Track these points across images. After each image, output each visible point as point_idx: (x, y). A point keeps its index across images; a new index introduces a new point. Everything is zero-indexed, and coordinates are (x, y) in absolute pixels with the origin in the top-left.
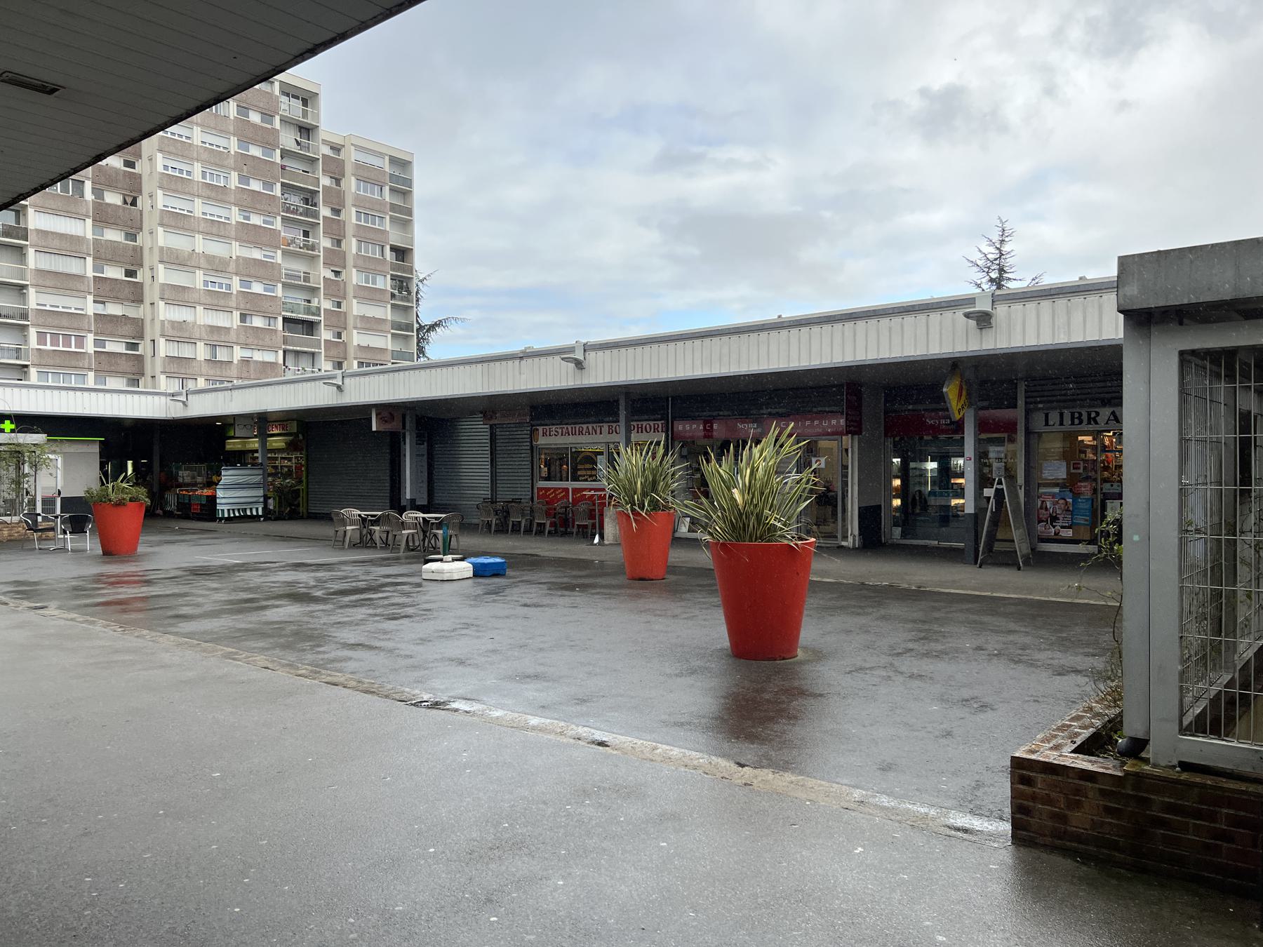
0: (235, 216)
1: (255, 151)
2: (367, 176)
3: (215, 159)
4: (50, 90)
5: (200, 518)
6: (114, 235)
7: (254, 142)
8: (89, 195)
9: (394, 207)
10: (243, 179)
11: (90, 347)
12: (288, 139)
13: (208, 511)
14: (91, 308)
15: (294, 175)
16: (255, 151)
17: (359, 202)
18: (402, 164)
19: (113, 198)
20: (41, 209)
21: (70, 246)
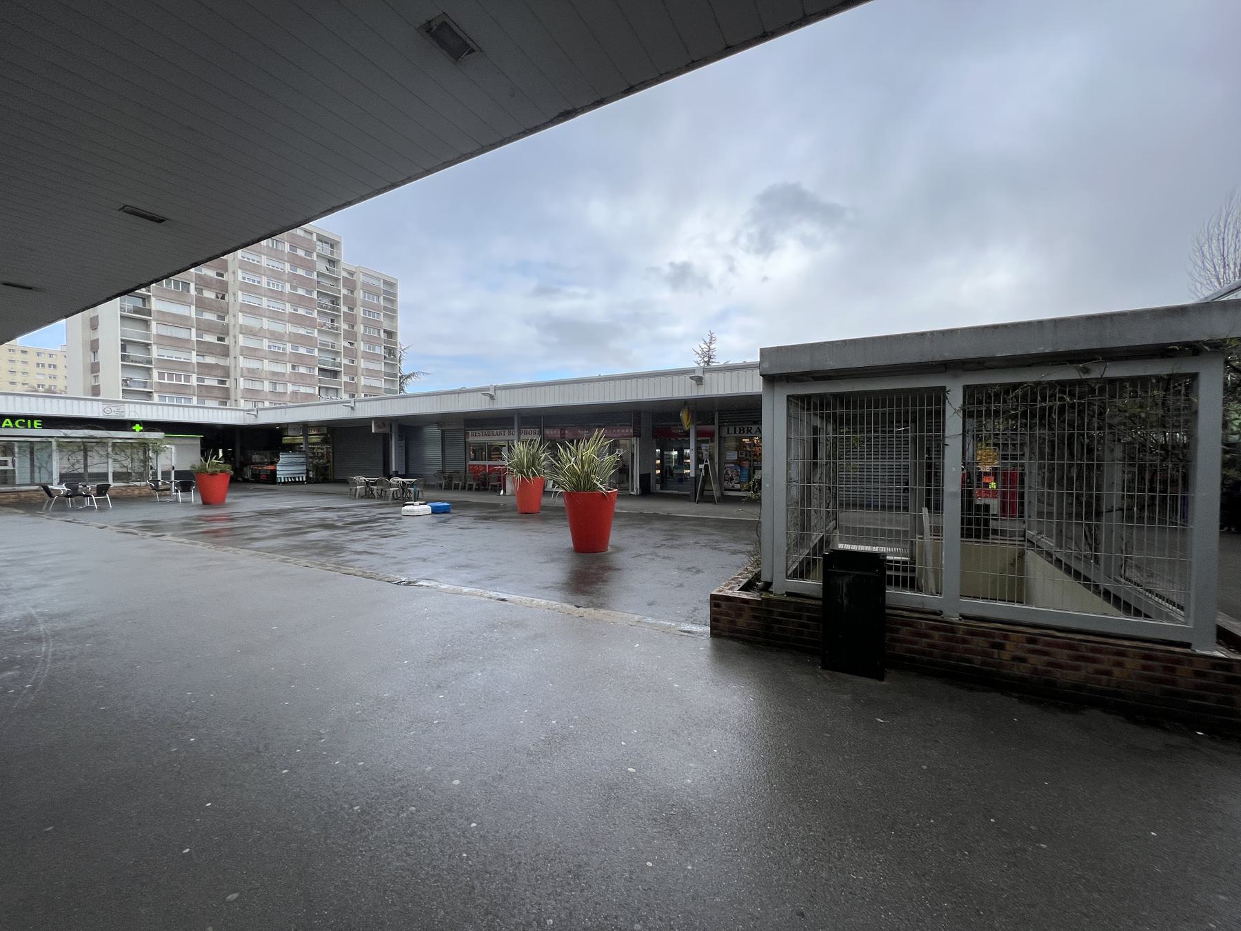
0: (288, 308)
1: (301, 272)
2: (369, 289)
3: (276, 275)
6: (209, 316)
7: (301, 266)
12: (322, 266)
13: (272, 478)
14: (194, 358)
16: (301, 272)
17: (364, 304)
18: (391, 284)
19: (209, 294)
20: (159, 298)
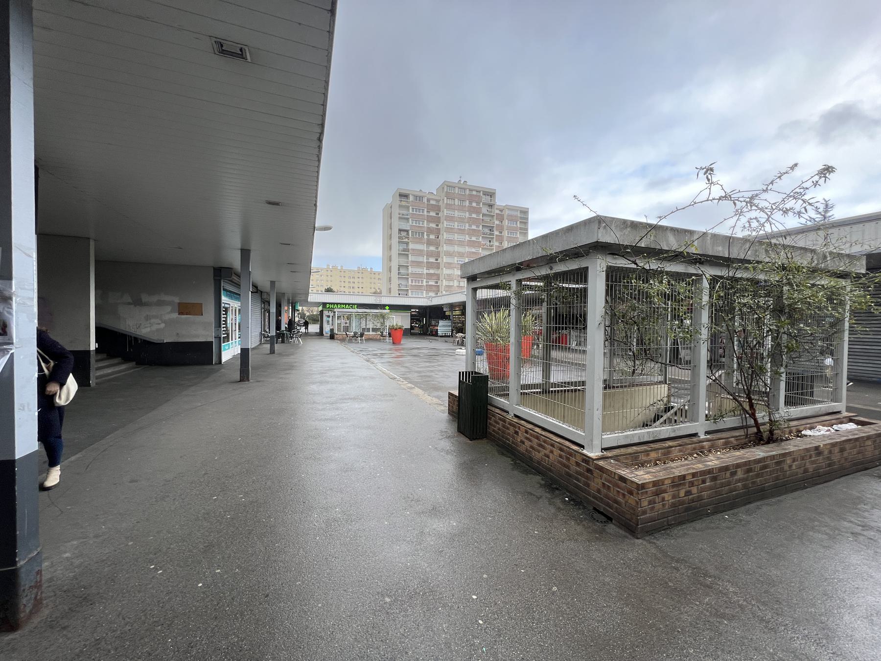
0: (467, 238)
1: (474, 216)
2: (512, 219)
3: (461, 220)
4: (277, 204)
5: (433, 335)
6: (432, 248)
7: (473, 212)
8: (425, 237)
9: (521, 229)
10: (470, 226)
11: (425, 284)
12: (485, 210)
13: (435, 334)
14: (425, 271)
15: (486, 222)
16: (474, 216)
17: (509, 228)
18: (525, 212)
19: (432, 237)
20: (413, 242)
21: (420, 253)
